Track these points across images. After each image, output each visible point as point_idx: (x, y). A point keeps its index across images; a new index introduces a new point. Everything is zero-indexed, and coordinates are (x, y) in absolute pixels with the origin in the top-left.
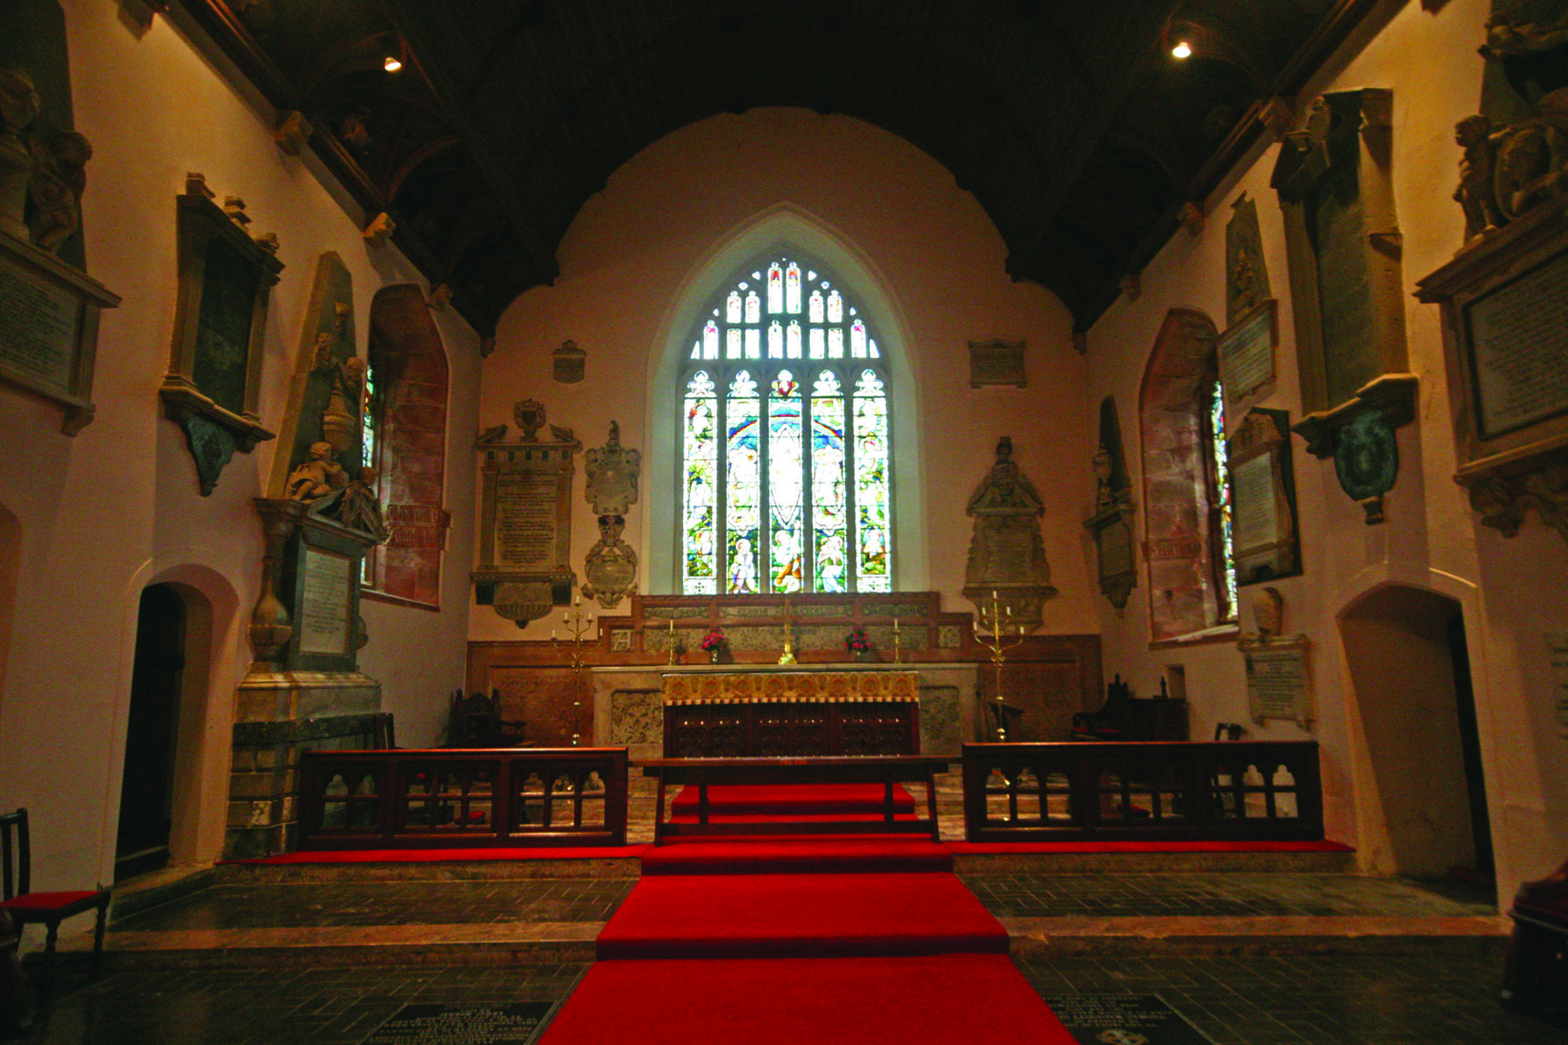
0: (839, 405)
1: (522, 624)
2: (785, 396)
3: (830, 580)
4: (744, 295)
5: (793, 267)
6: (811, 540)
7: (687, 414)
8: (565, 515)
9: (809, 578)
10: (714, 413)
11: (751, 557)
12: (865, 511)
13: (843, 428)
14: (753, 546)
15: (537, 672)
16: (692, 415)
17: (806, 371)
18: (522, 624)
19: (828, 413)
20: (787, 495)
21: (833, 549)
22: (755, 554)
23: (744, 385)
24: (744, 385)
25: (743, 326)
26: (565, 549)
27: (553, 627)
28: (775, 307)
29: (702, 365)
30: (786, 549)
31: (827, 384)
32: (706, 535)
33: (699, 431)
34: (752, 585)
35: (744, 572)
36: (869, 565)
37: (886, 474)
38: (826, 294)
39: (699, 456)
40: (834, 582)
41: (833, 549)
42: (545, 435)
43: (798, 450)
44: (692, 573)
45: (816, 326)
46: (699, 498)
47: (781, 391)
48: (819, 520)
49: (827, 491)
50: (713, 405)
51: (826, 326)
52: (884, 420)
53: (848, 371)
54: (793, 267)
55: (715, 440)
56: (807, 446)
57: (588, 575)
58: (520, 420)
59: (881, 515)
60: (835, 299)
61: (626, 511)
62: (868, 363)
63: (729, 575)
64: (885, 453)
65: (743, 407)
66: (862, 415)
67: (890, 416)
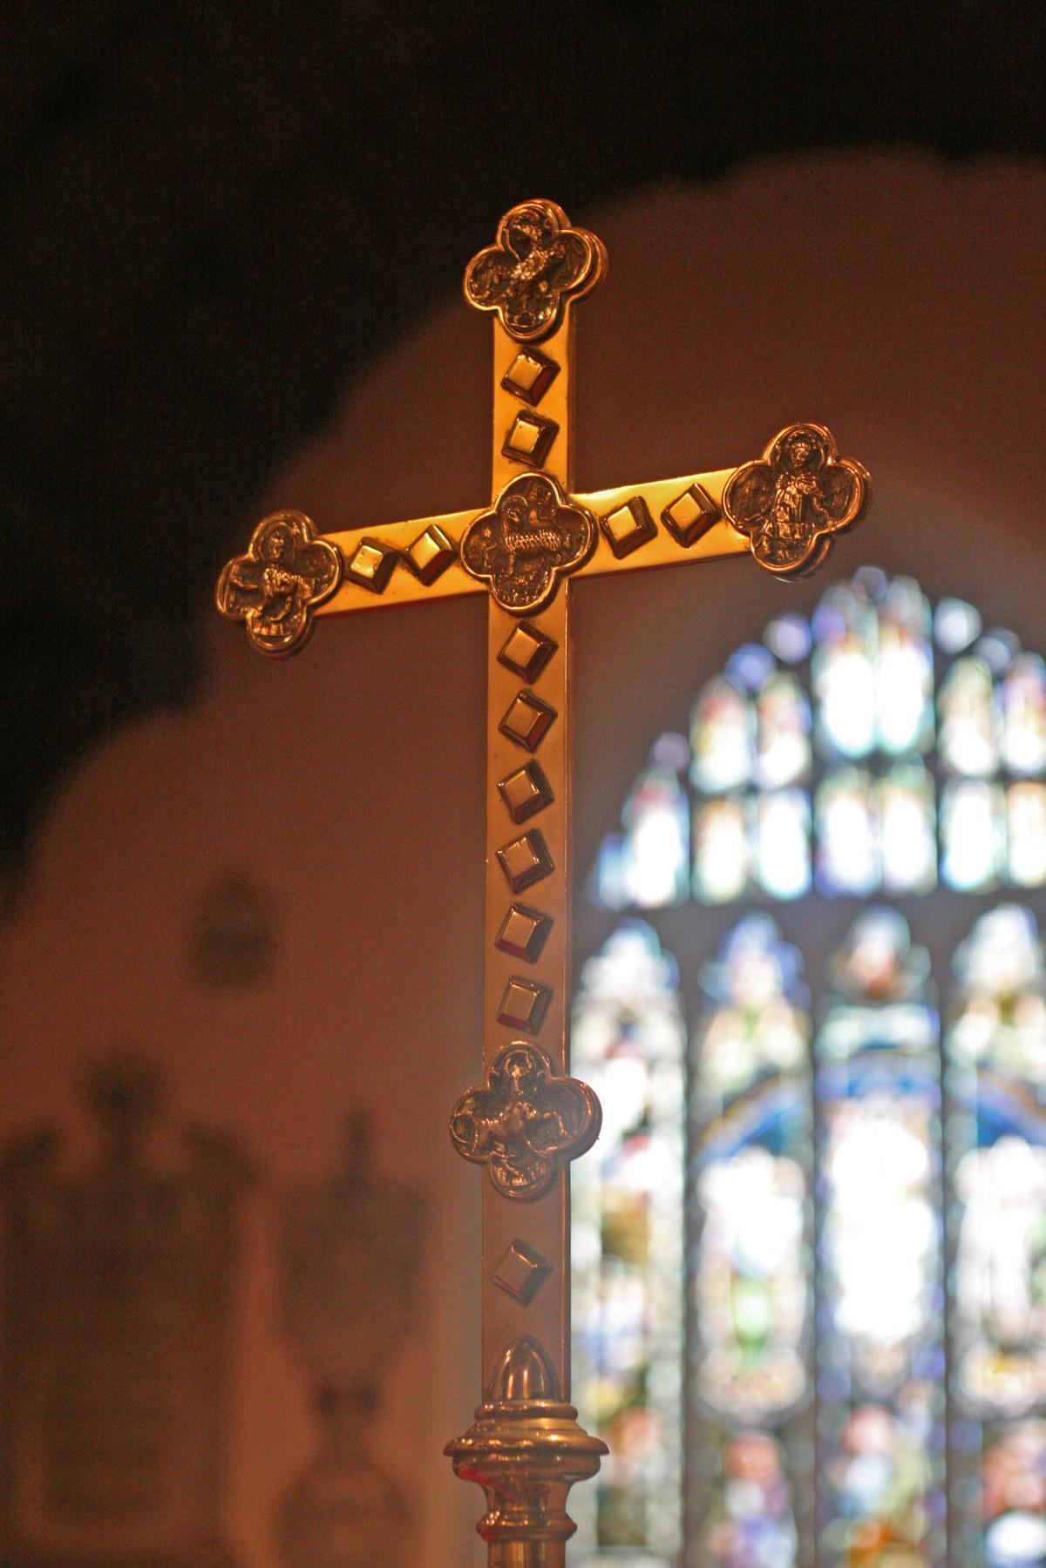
2: (876, 996)
23: (755, 970)
24: (755, 970)
29: (633, 915)
42: (164, 1151)
50: (662, 1034)
56: (945, 1151)
65: (758, 1027)
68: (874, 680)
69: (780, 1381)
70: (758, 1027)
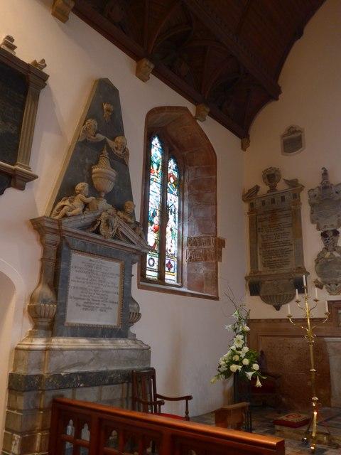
1: (278, 308)
8: (298, 234)
15: (289, 340)
18: (278, 308)
26: (300, 256)
27: (290, 310)
42: (281, 186)
57: (318, 274)
58: (266, 180)
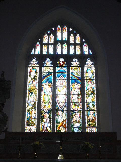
0: (79, 70)
2: (62, 66)
3: (76, 127)
4: (49, 35)
5: (65, 27)
6: (70, 114)
7: (29, 71)
9: (68, 127)
10: (38, 71)
11: (49, 120)
12: (88, 104)
13: (80, 76)
14: (50, 116)
16: (31, 72)
17: (68, 58)
19: (76, 72)
20: (61, 98)
21: (77, 117)
22: (50, 119)
23: (48, 62)
24: (48, 62)
25: (48, 44)
28: (59, 38)
29: (35, 56)
30: (61, 117)
31: (75, 63)
32: (33, 112)
33: (32, 77)
34: (49, 129)
35: (46, 124)
36: (90, 123)
37: (95, 92)
38: (75, 35)
39: (32, 84)
40: (77, 129)
41: (77, 117)
43: (65, 84)
44: (28, 125)
45: (72, 44)
46: (32, 99)
47: (60, 64)
48: (73, 107)
49: (75, 98)
50: (37, 68)
51: (75, 45)
52: (94, 75)
53: (82, 59)
54: (65, 27)
55: (38, 80)
59: (94, 106)
60: (78, 37)
61: (5, 101)
62: (88, 56)
63: (41, 126)
64: (95, 85)
65: (48, 69)
66: (87, 72)
67: (96, 73)
68: (62, 34)
69: (49, 106)
70: (48, 69)
